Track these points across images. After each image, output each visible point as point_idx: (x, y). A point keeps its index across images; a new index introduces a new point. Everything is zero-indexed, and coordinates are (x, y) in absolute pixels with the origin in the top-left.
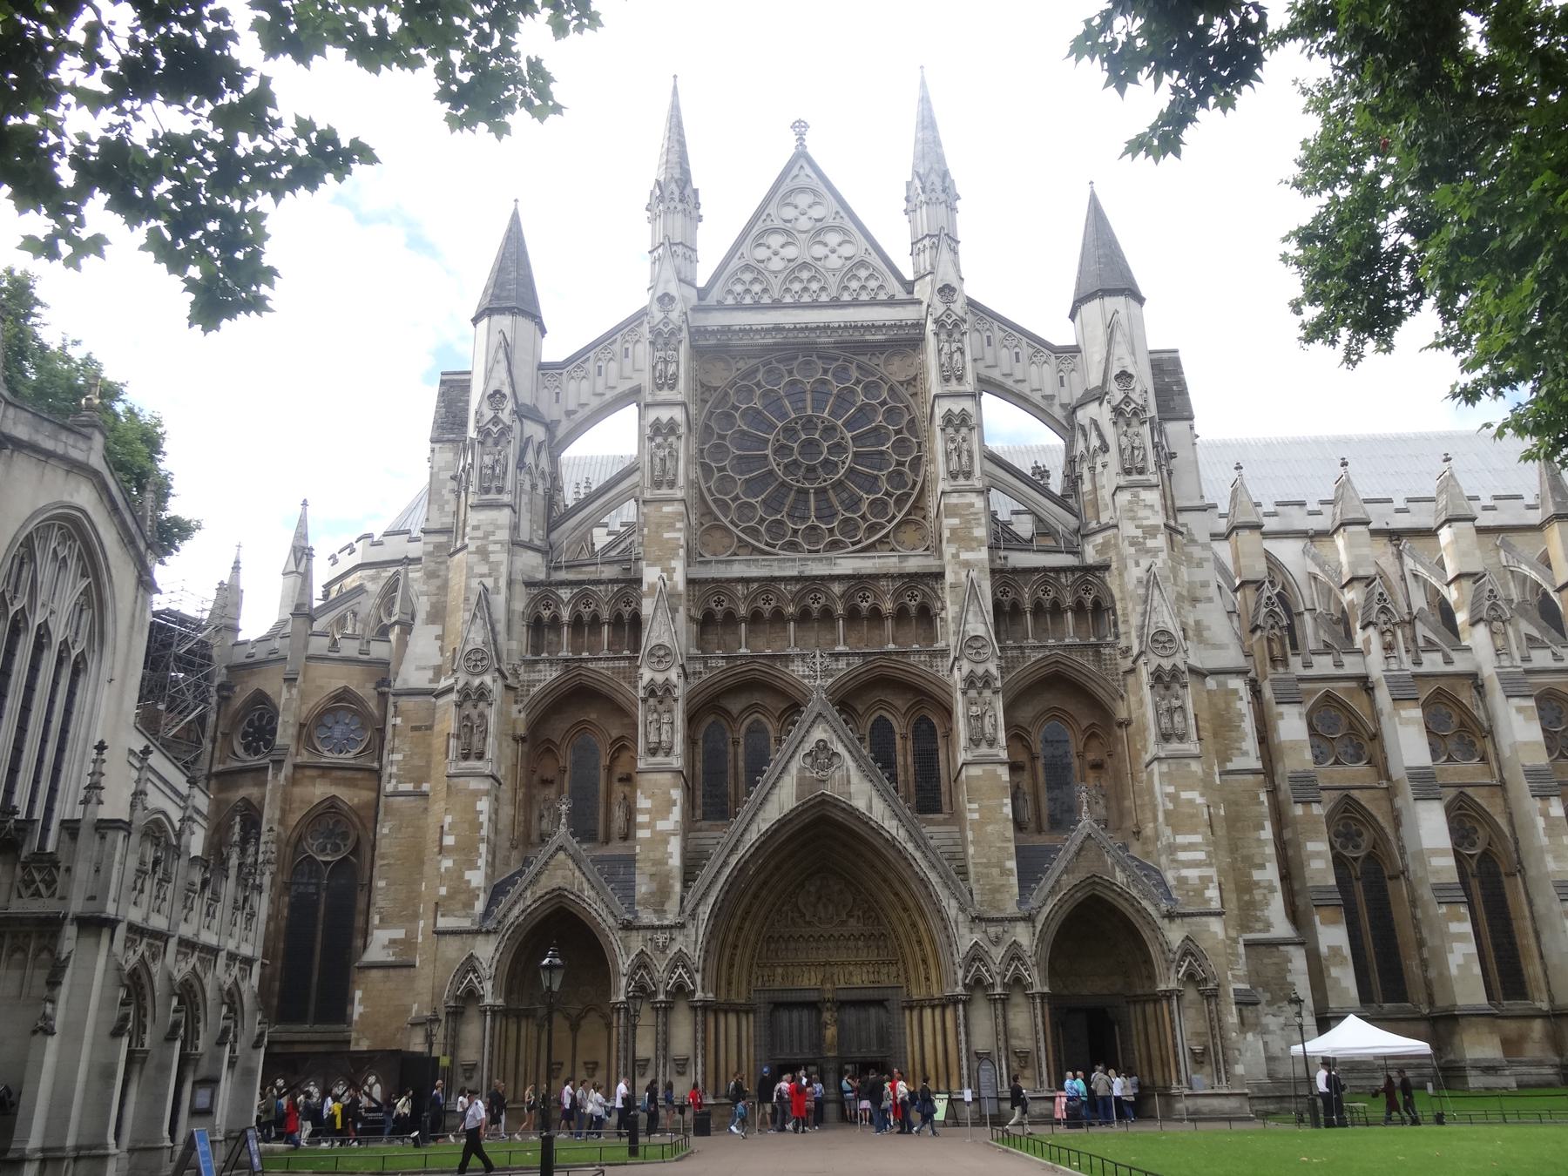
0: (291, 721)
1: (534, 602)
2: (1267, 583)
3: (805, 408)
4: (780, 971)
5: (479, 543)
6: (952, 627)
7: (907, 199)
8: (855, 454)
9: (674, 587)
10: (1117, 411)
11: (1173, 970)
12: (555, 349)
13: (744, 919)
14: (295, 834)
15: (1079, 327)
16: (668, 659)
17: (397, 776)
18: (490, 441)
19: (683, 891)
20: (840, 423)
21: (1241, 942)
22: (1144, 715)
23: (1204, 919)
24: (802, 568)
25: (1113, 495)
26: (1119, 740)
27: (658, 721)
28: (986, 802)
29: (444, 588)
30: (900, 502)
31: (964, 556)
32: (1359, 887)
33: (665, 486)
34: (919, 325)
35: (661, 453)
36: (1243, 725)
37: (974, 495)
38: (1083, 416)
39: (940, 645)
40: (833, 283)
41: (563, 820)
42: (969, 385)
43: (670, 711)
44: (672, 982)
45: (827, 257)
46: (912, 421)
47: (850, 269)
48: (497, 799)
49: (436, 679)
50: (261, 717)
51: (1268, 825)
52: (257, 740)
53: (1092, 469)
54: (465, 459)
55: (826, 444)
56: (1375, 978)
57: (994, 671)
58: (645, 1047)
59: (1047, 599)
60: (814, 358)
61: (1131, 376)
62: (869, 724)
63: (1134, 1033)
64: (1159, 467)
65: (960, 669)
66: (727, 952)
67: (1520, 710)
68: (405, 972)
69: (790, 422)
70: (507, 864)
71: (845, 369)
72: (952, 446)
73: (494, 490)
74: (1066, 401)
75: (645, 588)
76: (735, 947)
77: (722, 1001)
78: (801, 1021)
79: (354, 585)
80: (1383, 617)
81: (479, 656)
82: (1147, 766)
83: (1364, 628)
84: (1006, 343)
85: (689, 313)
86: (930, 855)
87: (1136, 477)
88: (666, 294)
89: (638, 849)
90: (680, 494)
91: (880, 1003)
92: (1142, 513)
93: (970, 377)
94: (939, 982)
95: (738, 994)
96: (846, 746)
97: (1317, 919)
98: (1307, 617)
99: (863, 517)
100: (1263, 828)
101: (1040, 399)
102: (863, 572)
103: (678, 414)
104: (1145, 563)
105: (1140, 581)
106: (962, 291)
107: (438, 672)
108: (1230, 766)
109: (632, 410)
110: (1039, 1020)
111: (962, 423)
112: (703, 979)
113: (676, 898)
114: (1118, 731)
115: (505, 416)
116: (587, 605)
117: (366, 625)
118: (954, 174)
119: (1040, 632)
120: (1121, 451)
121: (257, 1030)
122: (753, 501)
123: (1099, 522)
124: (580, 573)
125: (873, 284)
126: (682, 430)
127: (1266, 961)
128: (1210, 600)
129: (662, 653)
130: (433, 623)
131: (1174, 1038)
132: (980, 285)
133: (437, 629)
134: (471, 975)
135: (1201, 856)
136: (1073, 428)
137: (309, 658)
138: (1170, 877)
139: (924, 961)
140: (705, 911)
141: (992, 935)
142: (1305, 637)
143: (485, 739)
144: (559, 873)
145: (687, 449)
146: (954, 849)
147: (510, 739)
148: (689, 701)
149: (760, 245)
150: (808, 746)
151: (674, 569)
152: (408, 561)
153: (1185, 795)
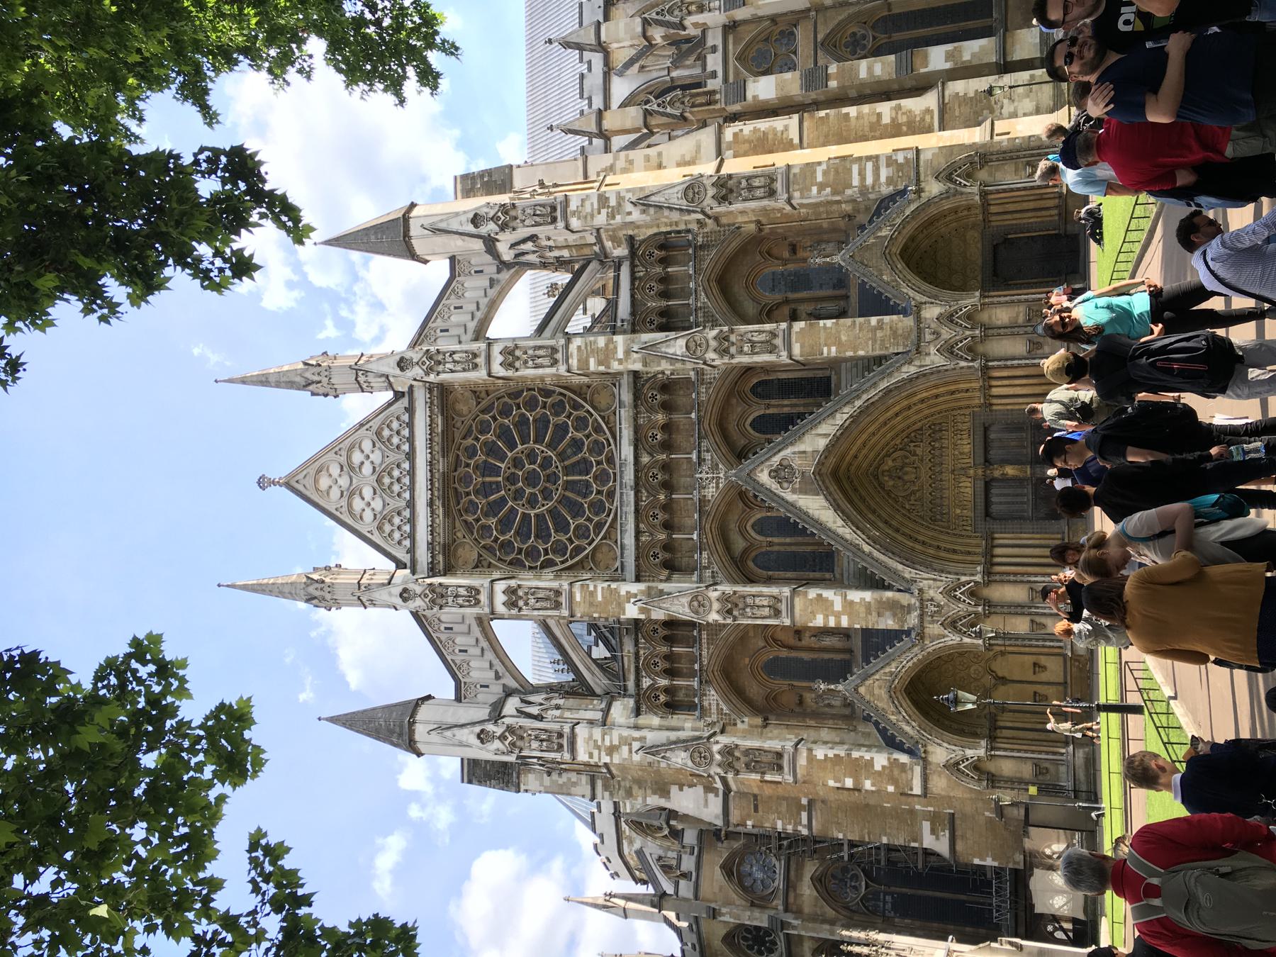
0: (748, 913)
1: (653, 710)
2: (647, 107)
3: (498, 483)
4: (958, 511)
5: (603, 753)
6: (679, 365)
7: (326, 395)
8: (535, 442)
9: (642, 592)
10: (503, 227)
12: (445, 688)
13: (916, 540)
14: (844, 913)
15: (434, 257)
16: (700, 598)
17: (796, 825)
18: (519, 743)
19: (892, 590)
20: (509, 454)
22: (753, 211)
23: (922, 163)
24: (628, 488)
25: (572, 232)
26: (772, 231)
27: (752, 607)
28: (822, 341)
29: (640, 783)
30: (576, 407)
31: (620, 355)
32: (897, 36)
33: (560, 599)
34: (430, 390)
35: (532, 602)
37: (571, 346)
38: (507, 255)
39: (692, 373)
40: (394, 457)
41: (833, 687)
42: (482, 345)
43: (744, 597)
44: (967, 601)
45: (372, 463)
46: (509, 395)
47: (383, 443)
48: (814, 742)
49: (715, 791)
50: (745, 939)
51: (845, 110)
52: (764, 943)
53: (551, 248)
54: (534, 764)
55: (527, 466)
56: (971, 24)
57: (715, 332)
58: (1020, 626)
59: (657, 287)
60: (456, 474)
61: (476, 215)
62: (757, 434)
63: (1014, 222)
64: (551, 193)
65: (713, 360)
66: (943, 554)
68: (958, 822)
69: (509, 495)
70: (869, 734)
71: (466, 449)
72: (531, 363)
73: (560, 741)
74: (494, 269)
75: (642, 617)
77: (983, 560)
78: (1001, 495)
79: (636, 859)
80: (676, 12)
81: (696, 755)
82: (794, 208)
83: (684, 28)
84: (446, 317)
86: (864, 388)
87: (558, 214)
88: (401, 595)
89: (857, 626)
90: (566, 586)
91: (986, 429)
92: (588, 209)
93: (475, 346)
94: (970, 381)
95: (978, 546)
96: (775, 454)
97: (922, 70)
98: (674, 74)
99: (588, 437)
100: (848, 114)
101: (493, 290)
102: (632, 438)
104: (629, 207)
105: (644, 212)
106: (403, 352)
107: (709, 789)
108: (796, 141)
109: (495, 624)
110: (1002, 299)
111: (511, 354)
112: (965, 575)
113: (898, 595)
114: (767, 231)
115: (499, 730)
116: (656, 664)
117: (669, 849)
118: (305, 358)
119: (685, 293)
120: (537, 224)
121: (1008, 947)
122: (572, 527)
123: (595, 244)
124: (629, 670)
125: (395, 425)
126: (513, 583)
127: (957, 113)
128: (660, 154)
129: (695, 604)
130: (669, 792)
131: (1018, 189)
132: (399, 339)
133: (674, 790)
134: (961, 767)
135: (869, 165)
136: (517, 263)
137: (696, 897)
138: (886, 190)
139: (953, 393)
140: (908, 573)
141: (932, 337)
142: (691, 76)
143: (765, 751)
144: (876, 691)
145: (529, 579)
146: (860, 367)
148: (735, 582)
149: (361, 518)
150: (773, 485)
151: (628, 592)
152: (617, 814)
153: (820, 178)
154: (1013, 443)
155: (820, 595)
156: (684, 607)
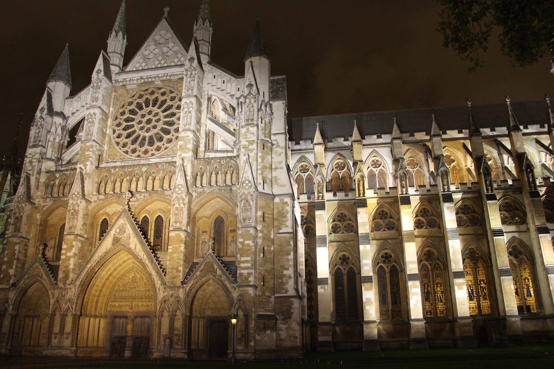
5: (30, 159)
9: (86, 171)
11: (233, 307)
13: (103, 287)
21: (273, 297)
23: (247, 288)
31: (183, 155)
36: (288, 215)
67: (448, 208)
73: (38, 141)
76: (99, 296)
85: (113, 76)
88: (99, 70)
91: (149, 317)
92: (249, 135)
97: (363, 288)
100: (290, 254)
103: (97, 111)
108: (281, 231)
112: (76, 306)
115: (44, 116)
140: (78, 283)
141: (170, 294)
144: (36, 270)
147: (35, 225)
153: (246, 242)
154: (143, 328)
155: (73, 246)
156: (76, 189)
